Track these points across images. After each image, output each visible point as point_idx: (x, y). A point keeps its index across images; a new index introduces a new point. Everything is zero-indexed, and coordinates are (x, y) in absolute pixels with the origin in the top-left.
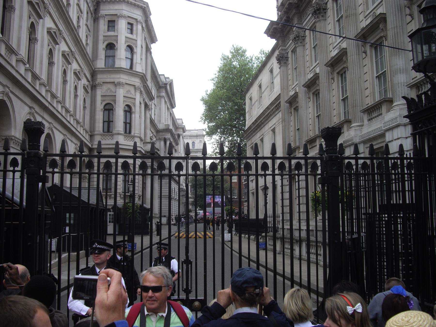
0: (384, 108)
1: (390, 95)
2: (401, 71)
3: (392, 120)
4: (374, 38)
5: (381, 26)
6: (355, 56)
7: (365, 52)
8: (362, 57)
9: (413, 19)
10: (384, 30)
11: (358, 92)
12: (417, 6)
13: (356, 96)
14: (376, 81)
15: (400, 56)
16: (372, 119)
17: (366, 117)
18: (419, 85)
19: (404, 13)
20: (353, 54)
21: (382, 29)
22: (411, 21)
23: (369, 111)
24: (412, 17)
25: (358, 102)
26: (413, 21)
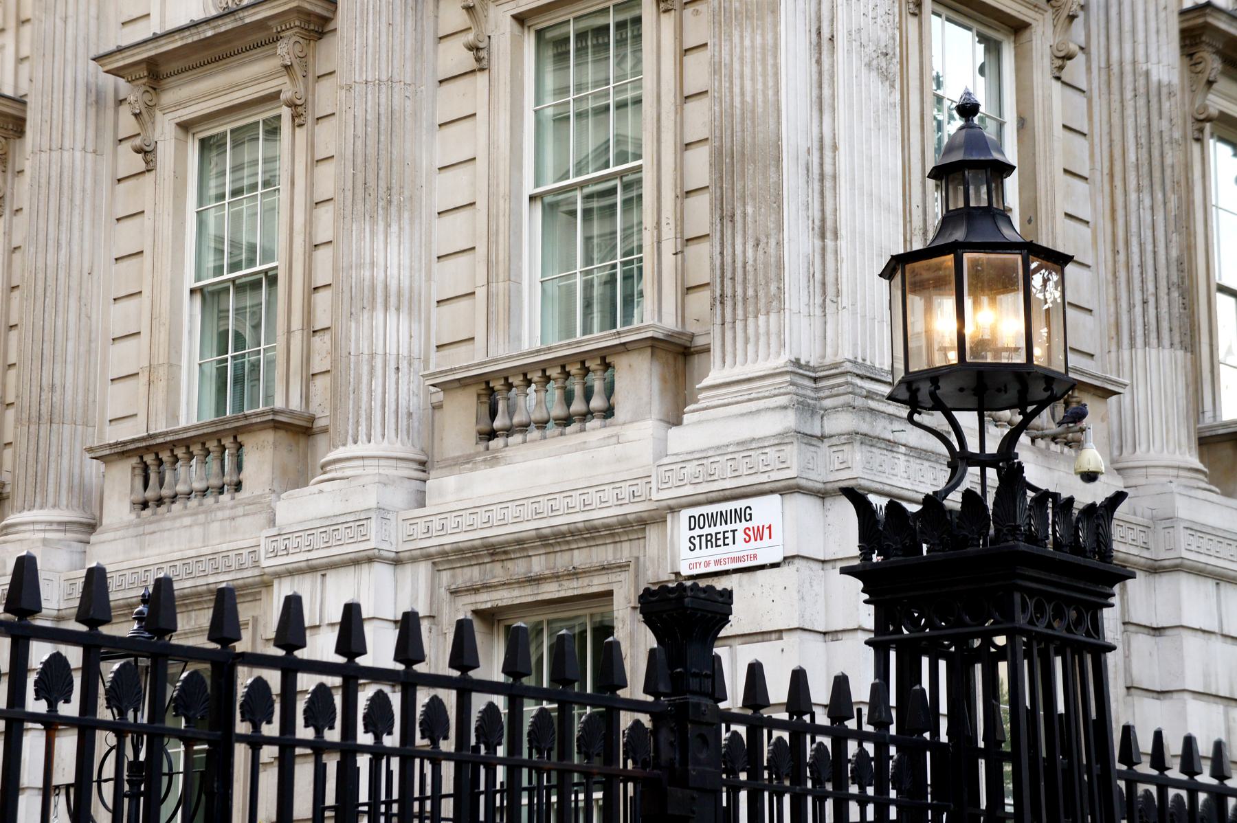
0: (261, 460)
1: (286, 397)
2: (393, 300)
3: (331, 526)
4: (215, 94)
5: (286, 50)
6: (78, 154)
7: (146, 152)
8: (115, 169)
9: (482, 70)
10: (297, 69)
11: (71, 344)
12: (515, 17)
13: (58, 367)
14: (191, 311)
15: (394, 228)
16: (160, 501)
17: (119, 486)
18: (497, 385)
19: (428, 25)
20: (67, 145)
21: (287, 68)
22: (473, 71)
23: (149, 459)
24: (478, 60)
25: (69, 397)
26: (482, 78)
